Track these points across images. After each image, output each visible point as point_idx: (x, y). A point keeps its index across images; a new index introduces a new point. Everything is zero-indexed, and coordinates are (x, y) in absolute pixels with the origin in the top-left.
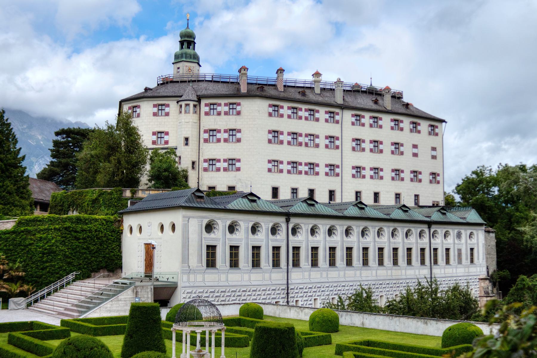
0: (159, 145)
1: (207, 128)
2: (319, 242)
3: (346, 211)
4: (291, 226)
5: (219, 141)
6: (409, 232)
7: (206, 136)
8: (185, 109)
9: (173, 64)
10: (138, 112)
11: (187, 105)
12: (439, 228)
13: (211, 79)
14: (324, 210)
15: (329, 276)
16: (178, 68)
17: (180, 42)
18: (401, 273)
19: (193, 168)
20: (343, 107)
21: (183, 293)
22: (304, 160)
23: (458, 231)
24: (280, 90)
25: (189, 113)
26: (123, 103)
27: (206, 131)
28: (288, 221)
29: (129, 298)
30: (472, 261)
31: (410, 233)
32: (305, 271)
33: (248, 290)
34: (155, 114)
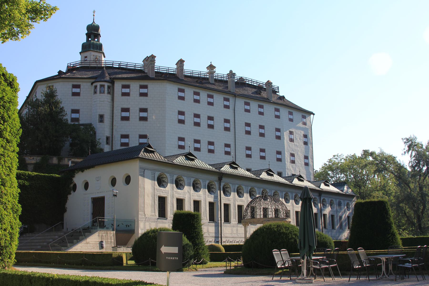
8: (100, 90)
9: (80, 53)
11: (102, 86)
12: (326, 197)
13: (118, 66)
16: (86, 57)
17: (86, 34)
19: (107, 143)
20: (235, 95)
23: (339, 201)
24: (181, 78)
25: (104, 93)
26: (38, 84)
28: (220, 179)
29: (96, 241)
32: (234, 227)
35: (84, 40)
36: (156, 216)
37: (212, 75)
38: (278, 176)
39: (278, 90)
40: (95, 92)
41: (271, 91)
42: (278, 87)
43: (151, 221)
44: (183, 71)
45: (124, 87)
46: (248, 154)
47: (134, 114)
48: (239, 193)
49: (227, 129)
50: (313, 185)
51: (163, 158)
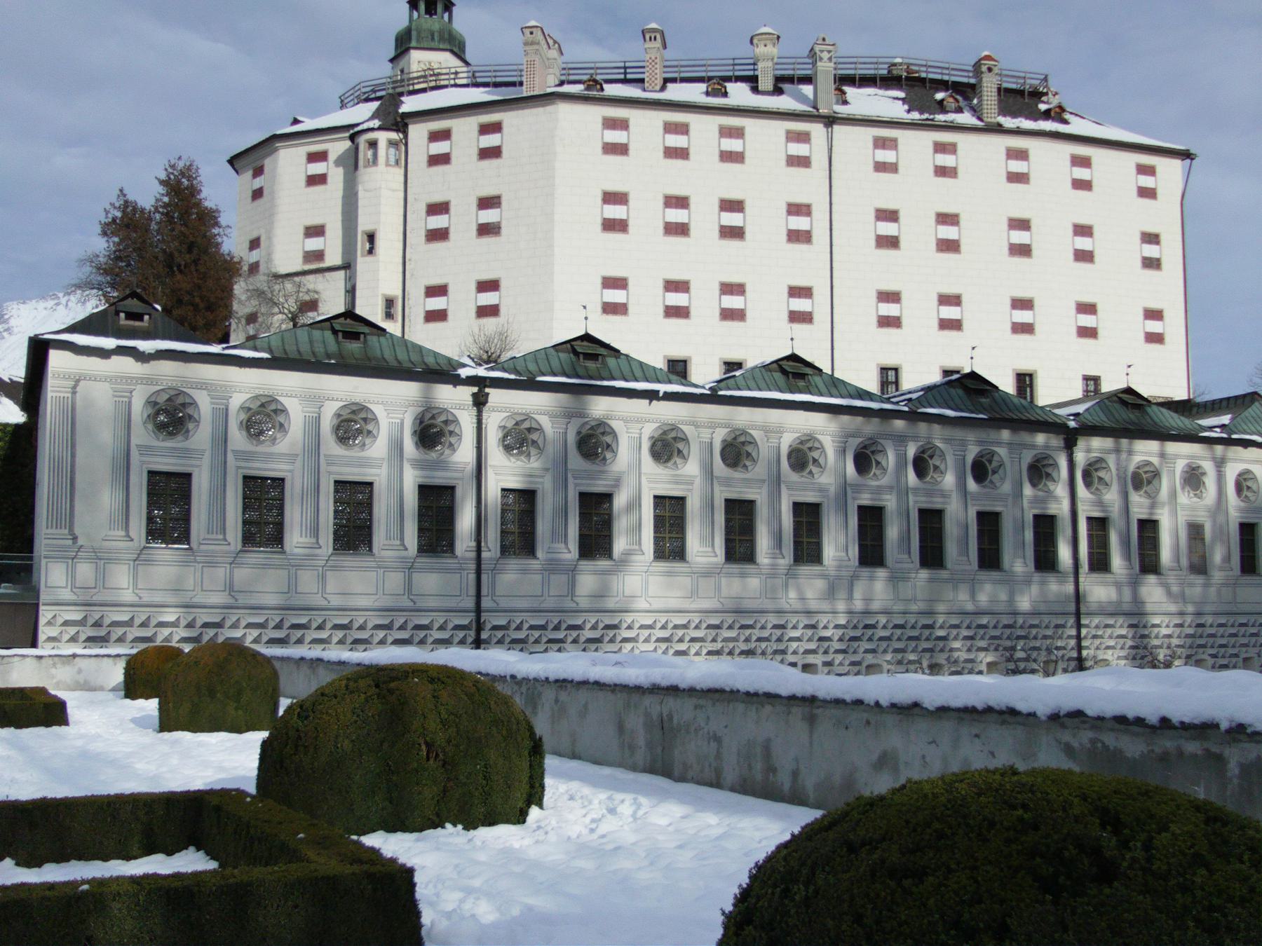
4: (494, 421)
9: (392, 61)
21: (49, 623)
30: (1248, 566)
31: (994, 464)
33: (315, 625)
36: (229, 544)
41: (991, 92)
43: (103, 559)
45: (435, 136)
46: (888, 317)
47: (463, 219)
49: (798, 237)
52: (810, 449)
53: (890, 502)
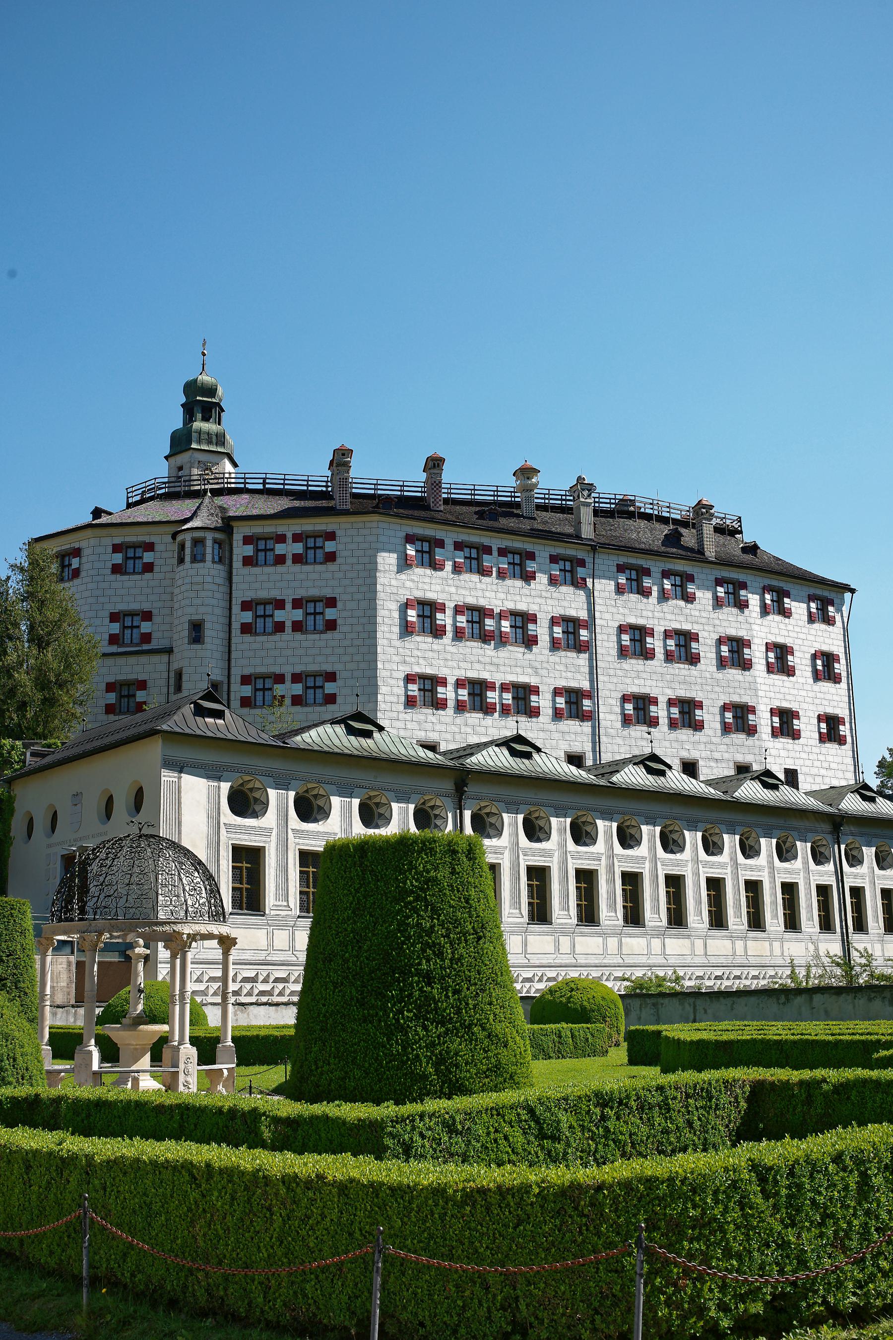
0: (128, 646)
1: (249, 596)
2: (547, 854)
3: (618, 775)
5: (279, 627)
6: (785, 843)
7: (248, 617)
8: (192, 552)
10: (73, 567)
13: (261, 487)
14: (560, 770)
15: (578, 949)
16: (180, 468)
18: (771, 950)
22: (498, 677)
25: (203, 560)
27: (246, 606)
31: (788, 844)
34: (117, 569)
35: (177, 422)
37: (527, 494)
38: (685, 776)
39: (740, 526)
40: (181, 561)
42: (740, 518)
44: (440, 487)
48: (538, 829)
50: (812, 799)
51: (253, 732)
52: (671, 832)
53: (646, 871)
